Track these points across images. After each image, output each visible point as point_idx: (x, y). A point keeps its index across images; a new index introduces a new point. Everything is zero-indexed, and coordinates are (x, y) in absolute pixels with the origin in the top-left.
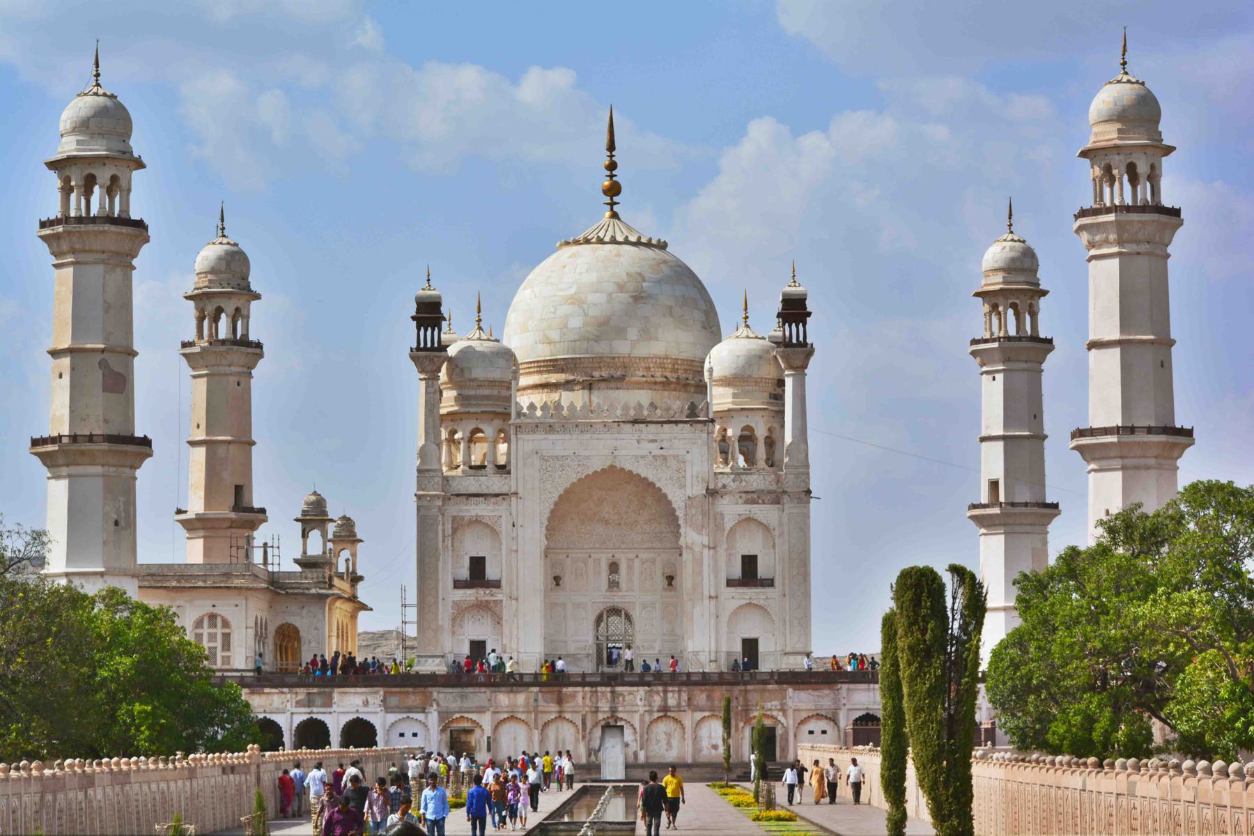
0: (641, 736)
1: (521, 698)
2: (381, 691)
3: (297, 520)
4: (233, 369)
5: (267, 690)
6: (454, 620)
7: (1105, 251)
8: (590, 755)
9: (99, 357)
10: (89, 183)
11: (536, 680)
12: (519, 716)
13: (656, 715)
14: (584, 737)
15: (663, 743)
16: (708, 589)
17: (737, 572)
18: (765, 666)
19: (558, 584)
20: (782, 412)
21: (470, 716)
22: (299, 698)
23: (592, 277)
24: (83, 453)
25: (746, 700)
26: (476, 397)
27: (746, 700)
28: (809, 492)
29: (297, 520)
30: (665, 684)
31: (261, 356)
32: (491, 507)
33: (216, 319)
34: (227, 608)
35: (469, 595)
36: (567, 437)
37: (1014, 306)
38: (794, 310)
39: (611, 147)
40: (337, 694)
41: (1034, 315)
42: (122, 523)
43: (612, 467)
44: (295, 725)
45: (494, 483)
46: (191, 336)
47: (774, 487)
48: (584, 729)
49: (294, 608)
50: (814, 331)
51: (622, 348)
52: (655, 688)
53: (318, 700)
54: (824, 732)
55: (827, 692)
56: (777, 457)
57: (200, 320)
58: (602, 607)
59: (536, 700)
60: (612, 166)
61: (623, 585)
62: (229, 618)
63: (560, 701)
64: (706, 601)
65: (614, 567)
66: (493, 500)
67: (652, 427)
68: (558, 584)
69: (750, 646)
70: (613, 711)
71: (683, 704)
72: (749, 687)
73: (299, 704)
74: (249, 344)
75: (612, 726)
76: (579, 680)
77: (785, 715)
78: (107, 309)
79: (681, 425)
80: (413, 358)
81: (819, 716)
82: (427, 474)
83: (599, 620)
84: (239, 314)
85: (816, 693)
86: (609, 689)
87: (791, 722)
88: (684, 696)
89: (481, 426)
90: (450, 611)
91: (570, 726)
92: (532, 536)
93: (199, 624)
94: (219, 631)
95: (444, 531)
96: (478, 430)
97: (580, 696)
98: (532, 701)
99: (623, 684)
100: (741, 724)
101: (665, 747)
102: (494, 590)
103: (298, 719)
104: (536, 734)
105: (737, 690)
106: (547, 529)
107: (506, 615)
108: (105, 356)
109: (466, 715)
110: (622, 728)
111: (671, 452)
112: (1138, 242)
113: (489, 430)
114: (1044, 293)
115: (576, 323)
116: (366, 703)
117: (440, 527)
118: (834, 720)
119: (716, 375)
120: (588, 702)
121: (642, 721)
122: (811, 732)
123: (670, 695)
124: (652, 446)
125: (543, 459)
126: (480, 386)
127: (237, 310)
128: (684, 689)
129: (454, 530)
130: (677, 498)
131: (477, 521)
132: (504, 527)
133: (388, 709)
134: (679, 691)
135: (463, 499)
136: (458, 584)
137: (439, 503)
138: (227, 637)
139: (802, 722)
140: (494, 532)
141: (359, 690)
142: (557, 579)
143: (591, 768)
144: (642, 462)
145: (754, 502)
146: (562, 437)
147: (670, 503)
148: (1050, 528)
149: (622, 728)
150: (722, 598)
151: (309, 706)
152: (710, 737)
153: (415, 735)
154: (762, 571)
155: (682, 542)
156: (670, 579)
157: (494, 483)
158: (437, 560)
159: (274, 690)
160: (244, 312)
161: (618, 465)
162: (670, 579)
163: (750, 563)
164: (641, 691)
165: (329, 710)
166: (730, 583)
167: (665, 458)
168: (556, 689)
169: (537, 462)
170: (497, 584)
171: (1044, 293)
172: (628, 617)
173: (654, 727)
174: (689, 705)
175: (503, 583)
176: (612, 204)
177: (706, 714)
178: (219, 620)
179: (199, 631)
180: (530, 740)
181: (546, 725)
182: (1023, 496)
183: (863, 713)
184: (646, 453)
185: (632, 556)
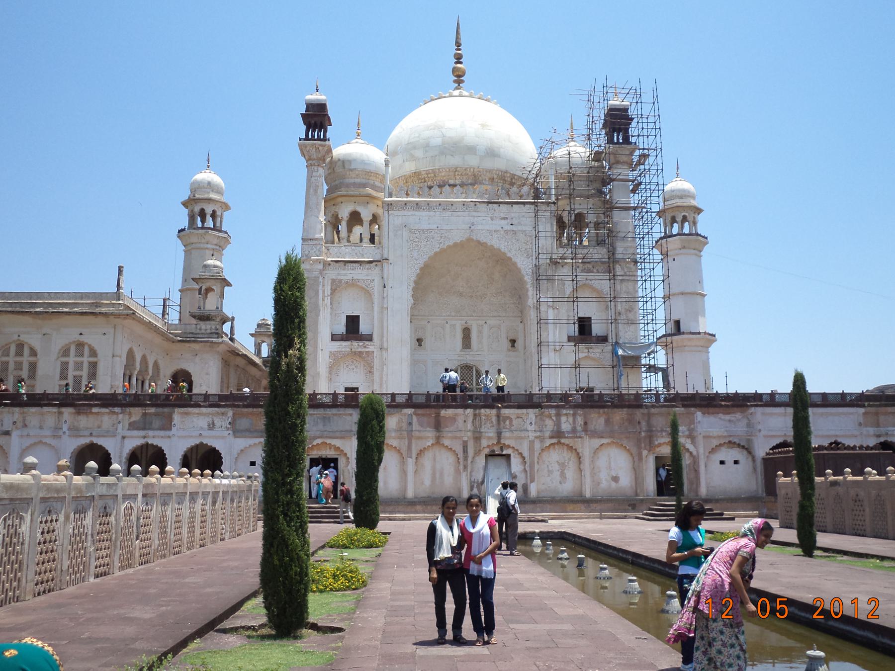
2: (230, 412)
4: (209, 246)
5: (95, 410)
6: (331, 367)
8: (472, 488)
11: (411, 401)
13: (548, 442)
14: (465, 467)
15: (556, 475)
19: (420, 345)
21: (334, 442)
22: (133, 419)
32: (365, 272)
33: (203, 221)
34: (96, 336)
35: (344, 346)
36: (432, 213)
38: (618, 122)
39: (458, 45)
40: (178, 415)
43: (469, 240)
45: (368, 252)
46: (185, 223)
51: (473, 161)
52: (547, 411)
53: (157, 423)
54: (736, 462)
55: (738, 415)
57: (192, 218)
59: (410, 424)
60: (458, 59)
62: (96, 348)
63: (438, 426)
66: (368, 266)
67: (504, 207)
68: (420, 345)
71: (579, 428)
72: (653, 410)
73: (133, 426)
75: (498, 455)
77: (693, 442)
79: (527, 206)
81: (731, 444)
82: (310, 242)
84: (214, 215)
85: (728, 417)
86: (494, 411)
88: (580, 421)
89: (359, 209)
90: (328, 360)
92: (400, 296)
93: (66, 352)
94: (86, 359)
95: (324, 292)
96: (355, 218)
98: (405, 425)
100: (645, 453)
101: (558, 478)
102: (367, 343)
104: (411, 462)
106: (414, 290)
107: (376, 363)
109: (328, 441)
110: (508, 457)
111: (520, 228)
114: (698, 211)
116: (212, 426)
117: (321, 286)
118: (748, 449)
122: (722, 462)
123: (563, 419)
124: (503, 222)
125: (411, 231)
127: (214, 212)
128: (580, 412)
129: (333, 291)
130: (525, 265)
131: (352, 284)
133: (237, 432)
134: (574, 415)
135: (342, 264)
136: (334, 338)
137: (321, 267)
138: (93, 366)
139: (713, 451)
140: (368, 294)
141: (204, 410)
142: (419, 341)
144: (495, 235)
145: (589, 271)
146: (427, 213)
147: (519, 270)
148: (710, 349)
149: (508, 457)
151: (144, 429)
152: (610, 468)
154: (597, 329)
156: (513, 342)
157: (368, 252)
158: (317, 315)
159: (106, 410)
160: (219, 213)
161: (474, 238)
162: (513, 342)
164: (532, 413)
165: (167, 433)
167: (515, 232)
170: (369, 338)
173: (545, 454)
174: (585, 430)
175: (375, 337)
177: (605, 441)
178: (86, 349)
179: (65, 359)
180: (404, 472)
181: (421, 453)
184: (499, 228)
185: (481, 322)
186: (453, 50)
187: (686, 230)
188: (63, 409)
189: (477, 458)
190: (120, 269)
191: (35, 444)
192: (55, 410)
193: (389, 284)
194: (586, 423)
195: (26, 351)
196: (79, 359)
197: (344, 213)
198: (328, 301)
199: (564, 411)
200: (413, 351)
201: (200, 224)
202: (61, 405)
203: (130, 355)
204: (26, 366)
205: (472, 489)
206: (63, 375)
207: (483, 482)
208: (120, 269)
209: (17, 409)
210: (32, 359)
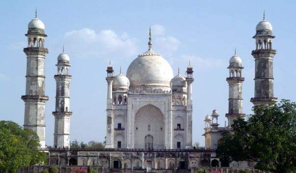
10: (35, 39)
18: (182, 148)
33: (62, 70)
37: (236, 71)
38: (190, 71)
41: (240, 72)
50: (194, 75)
61: (151, 129)
65: (149, 126)
69: (179, 144)
80: (107, 79)
83: (146, 137)
107: (125, 137)
114: (243, 68)
131: (120, 116)
142: (137, 128)
149: (151, 161)
154: (182, 128)
156: (162, 129)
162: (162, 129)
166: (175, 130)
171: (243, 68)
172: (152, 137)
176: (150, 47)
197: (117, 96)
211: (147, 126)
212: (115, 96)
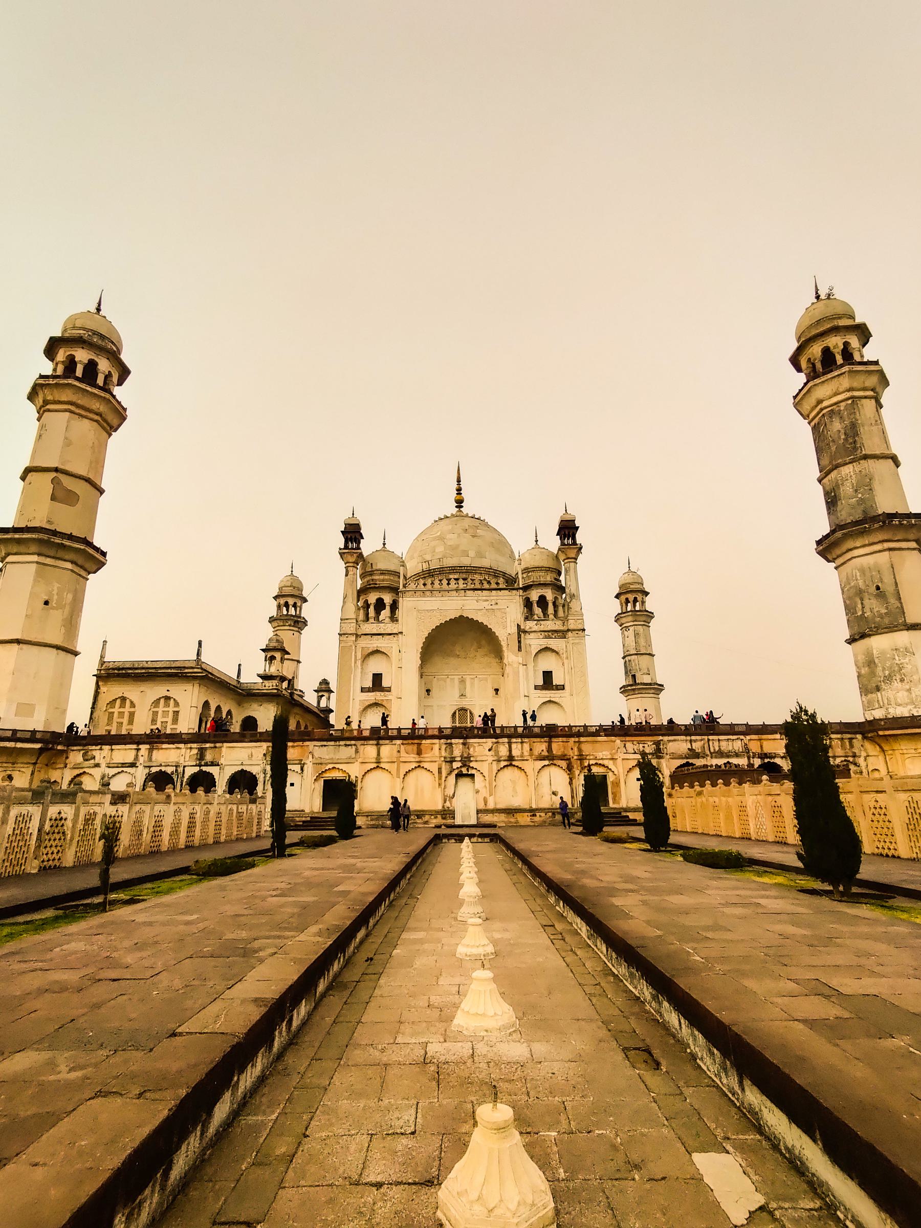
0: (490, 784)
1: (388, 750)
3: (263, 650)
5: (164, 746)
7: (835, 400)
9: (54, 474)
12: (382, 765)
13: (503, 764)
16: (523, 690)
17: (540, 682)
20: (562, 589)
23: (450, 527)
24: (19, 541)
25: (580, 750)
26: (379, 580)
27: (580, 750)
28: (584, 630)
29: (263, 650)
30: (509, 736)
31: (305, 623)
35: (372, 697)
38: (568, 529)
39: (459, 481)
41: (643, 603)
42: (53, 603)
43: (461, 616)
44: (187, 776)
45: (390, 627)
47: (562, 628)
48: (440, 778)
49: (255, 706)
51: (466, 561)
52: (500, 740)
56: (561, 613)
57: (279, 607)
58: (456, 708)
59: (399, 751)
60: (459, 490)
61: (468, 695)
63: (419, 753)
64: (523, 698)
70: (466, 761)
72: (582, 739)
74: (300, 617)
75: (464, 774)
76: (437, 733)
77: (615, 764)
78: (68, 443)
80: (341, 555)
86: (461, 741)
87: (621, 771)
88: (526, 747)
91: (428, 773)
93: (156, 703)
94: (171, 709)
97: (436, 747)
99: (475, 737)
103: (190, 771)
104: (399, 781)
105: (573, 739)
108: (62, 477)
109: (337, 766)
110: (472, 776)
112: (864, 389)
113: (388, 599)
114: (647, 594)
115: (440, 549)
119: (523, 566)
120: (444, 754)
121: (490, 770)
123: (514, 746)
126: (382, 574)
128: (526, 740)
131: (377, 652)
132: (394, 654)
134: (522, 743)
135: (369, 637)
136: (363, 690)
137: (354, 638)
138: (176, 713)
142: (428, 691)
143: (447, 813)
149: (472, 776)
150: (532, 696)
153: (292, 785)
154: (556, 681)
155: (505, 661)
156: (497, 690)
157: (390, 627)
159: (171, 746)
160: (299, 604)
162: (497, 690)
163: (548, 675)
164: (489, 742)
166: (536, 687)
168: (416, 741)
169: (415, 613)
170: (389, 690)
171: (647, 594)
173: (501, 773)
174: (531, 755)
177: (547, 762)
182: (647, 679)
183: (685, 761)
186: (456, 486)
187: (637, 608)
188: (141, 746)
189: (449, 777)
190: (200, 643)
191: (119, 773)
192: (135, 746)
193: (403, 651)
194: (531, 750)
195: (128, 701)
196: (166, 709)
197: (372, 598)
198: (359, 663)
199: (514, 740)
200: (420, 700)
201: (285, 612)
202: (138, 743)
203: (206, 705)
204: (126, 715)
205: (445, 802)
206: (154, 721)
207: (454, 795)
208: (200, 643)
209: (108, 747)
210: (132, 710)
211: (457, 682)
212: (366, 601)
